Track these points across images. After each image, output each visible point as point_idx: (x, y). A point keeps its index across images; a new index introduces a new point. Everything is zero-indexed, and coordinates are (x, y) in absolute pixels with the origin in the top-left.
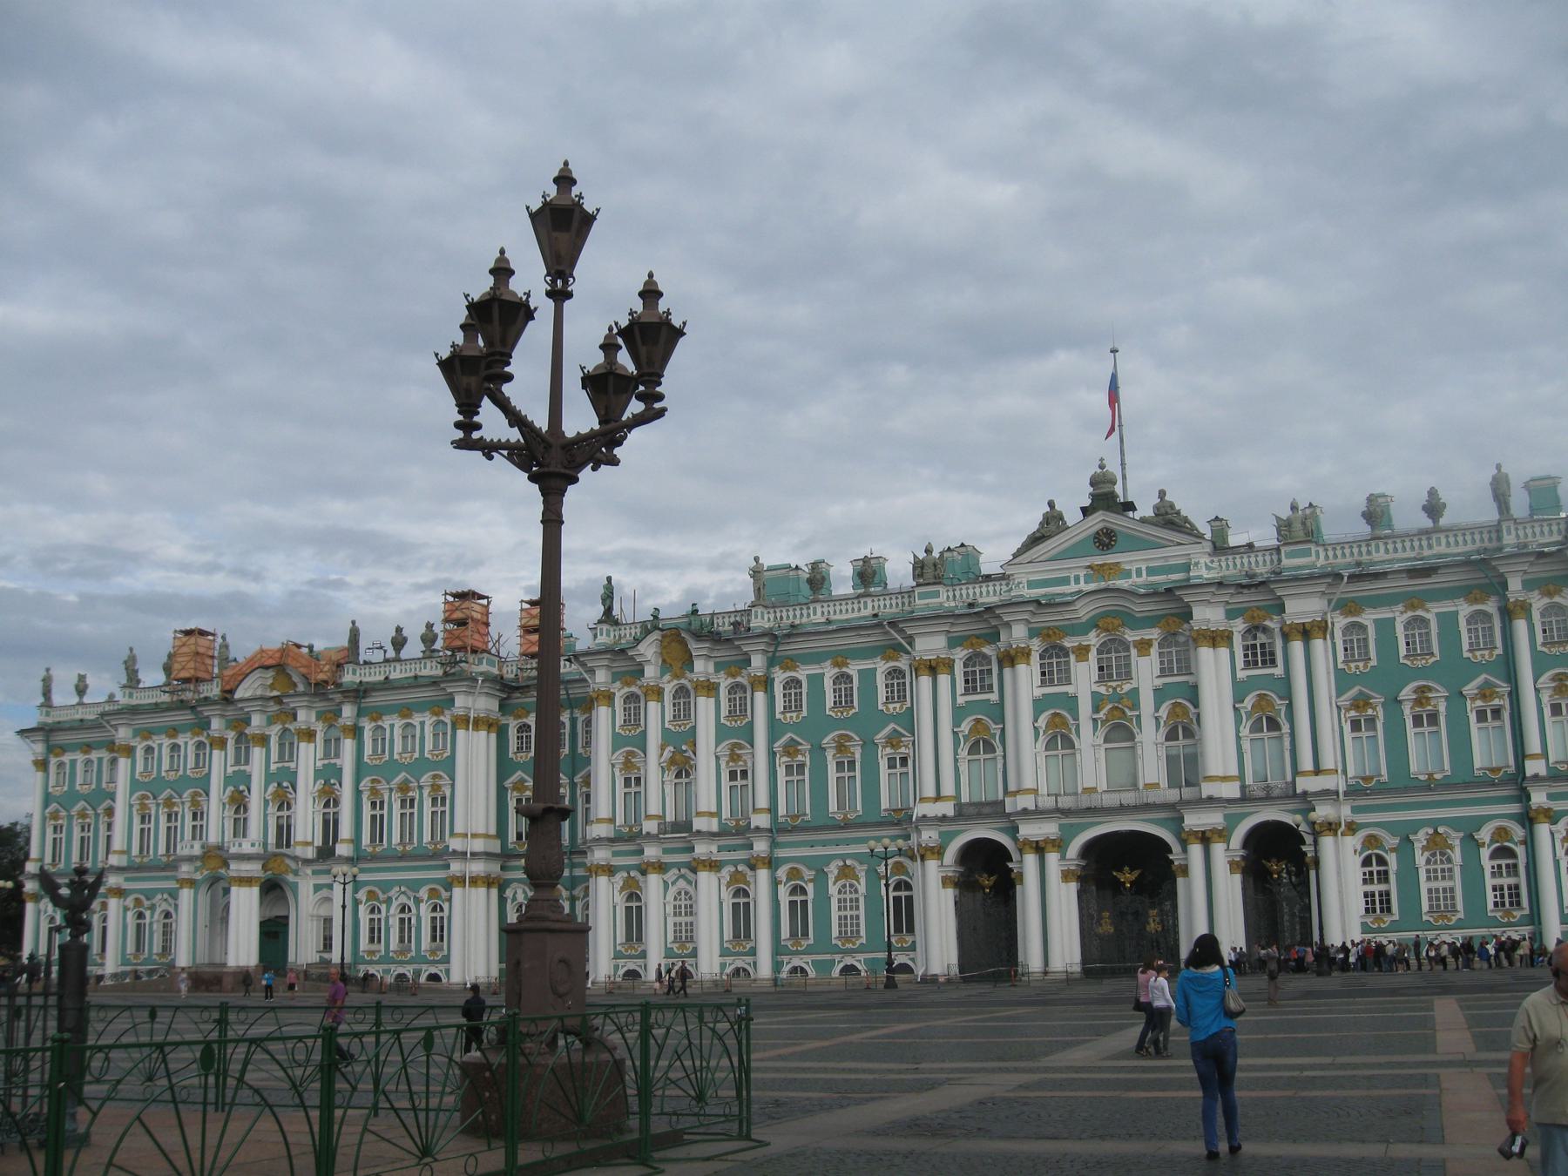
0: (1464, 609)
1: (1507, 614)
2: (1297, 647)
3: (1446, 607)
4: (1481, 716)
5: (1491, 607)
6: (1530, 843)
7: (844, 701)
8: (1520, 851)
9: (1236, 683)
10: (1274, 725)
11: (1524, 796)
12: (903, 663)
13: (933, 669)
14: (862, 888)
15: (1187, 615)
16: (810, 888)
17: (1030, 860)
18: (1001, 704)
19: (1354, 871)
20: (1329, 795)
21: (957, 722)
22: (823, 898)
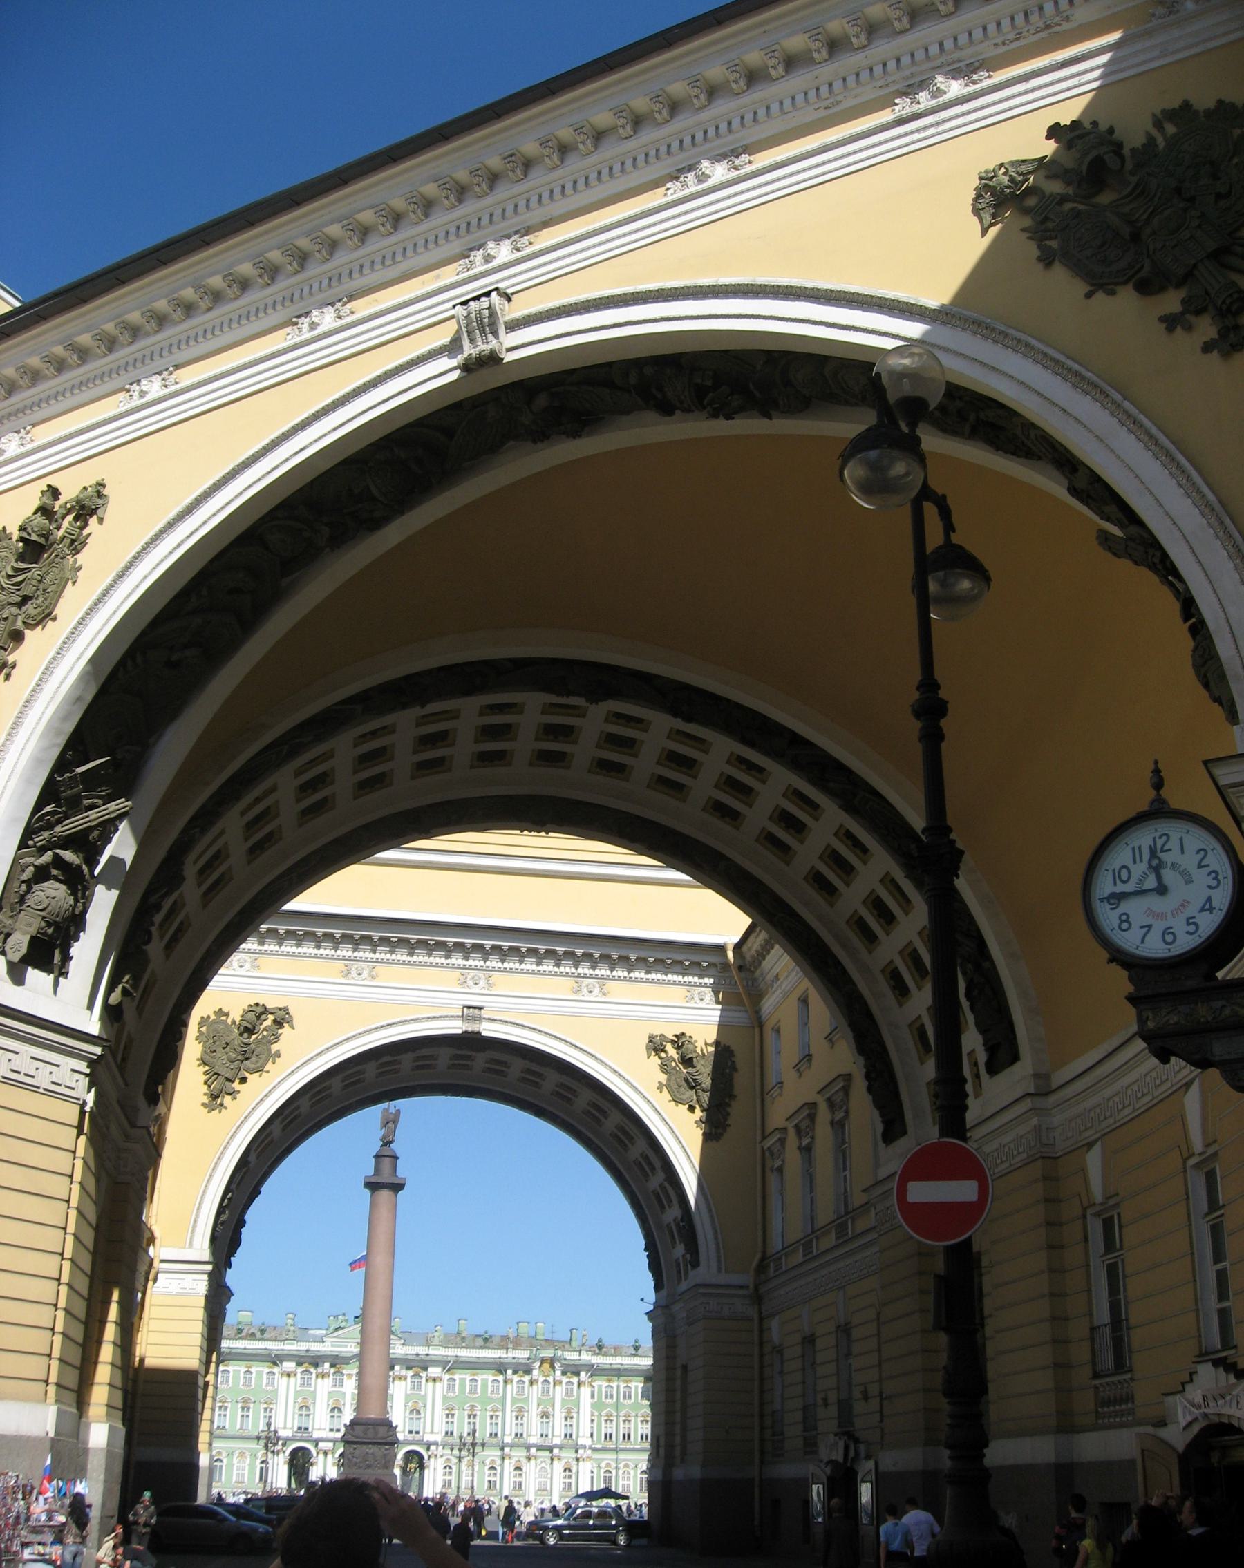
0: (491, 1378)
1: (506, 1382)
2: (431, 1384)
3: (485, 1377)
4: (492, 1417)
5: (501, 1378)
6: (502, 1465)
7: (247, 1384)
8: (499, 1469)
9: (407, 1395)
10: (418, 1412)
11: (502, 1449)
12: (276, 1370)
13: (289, 1375)
14: (248, 1461)
15: (392, 1368)
16: (225, 1460)
17: (321, 1456)
18: (314, 1392)
19: (440, 1470)
20: (436, 1444)
21: (296, 1398)
22: (231, 1465)
